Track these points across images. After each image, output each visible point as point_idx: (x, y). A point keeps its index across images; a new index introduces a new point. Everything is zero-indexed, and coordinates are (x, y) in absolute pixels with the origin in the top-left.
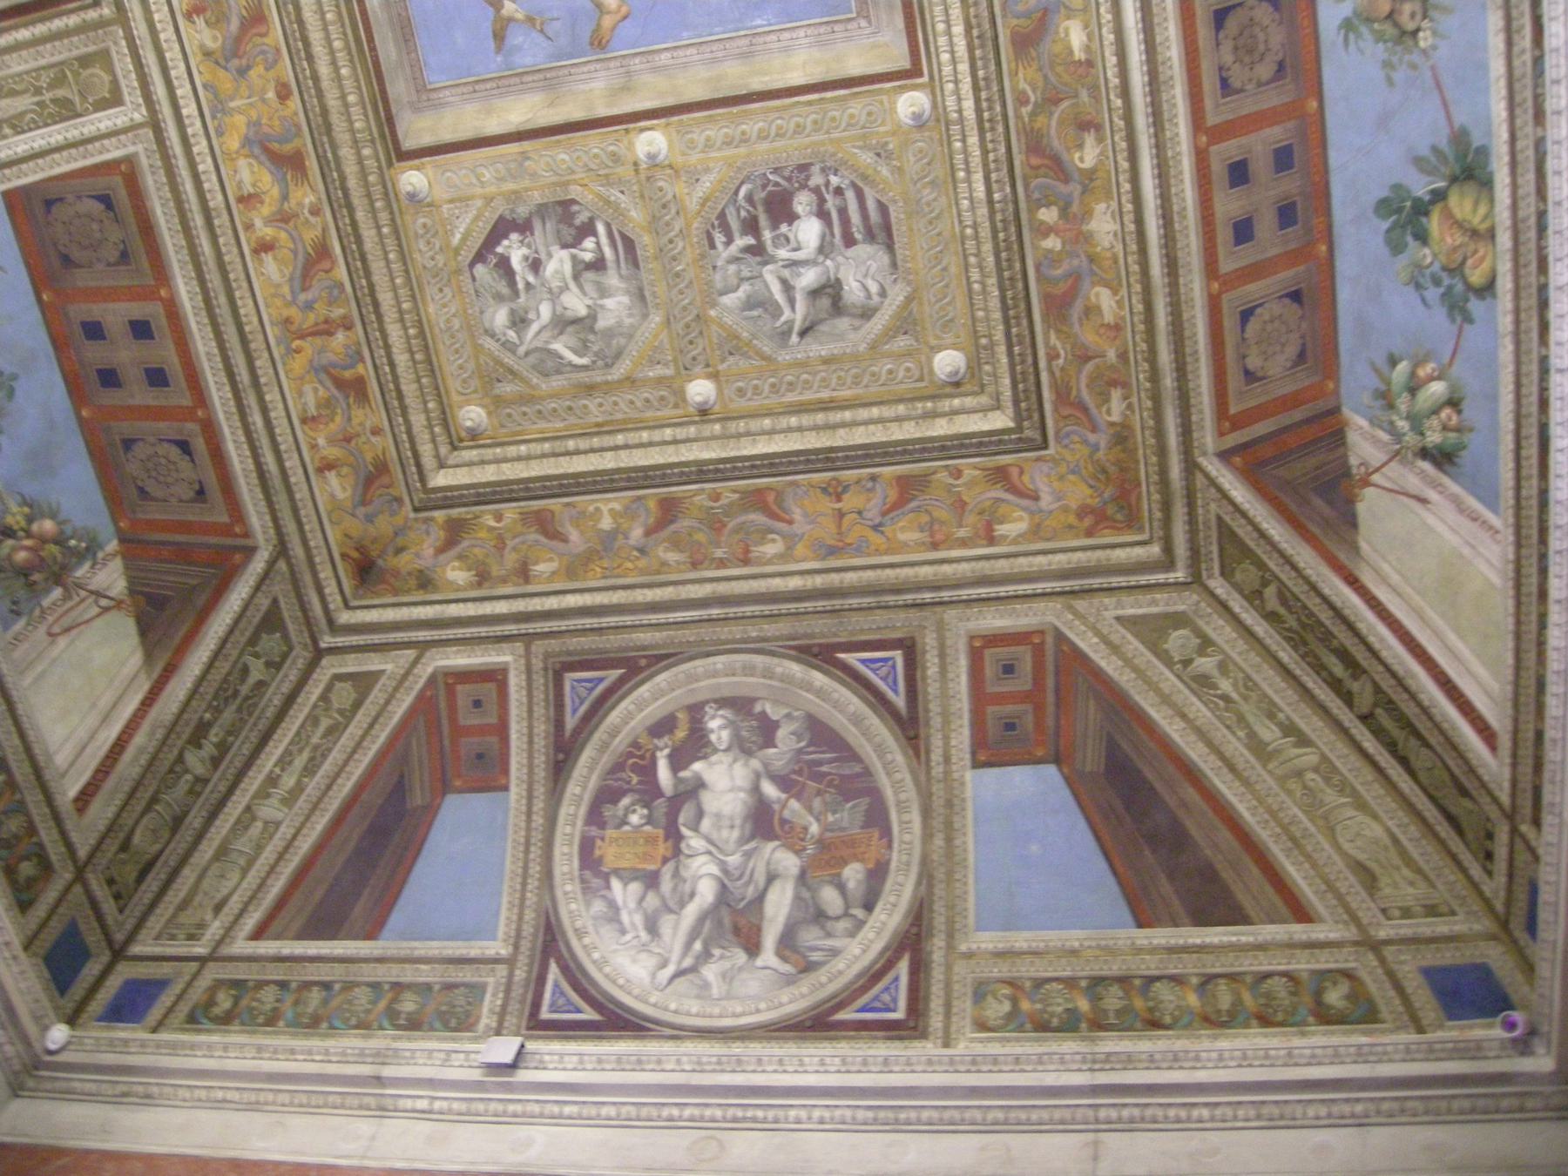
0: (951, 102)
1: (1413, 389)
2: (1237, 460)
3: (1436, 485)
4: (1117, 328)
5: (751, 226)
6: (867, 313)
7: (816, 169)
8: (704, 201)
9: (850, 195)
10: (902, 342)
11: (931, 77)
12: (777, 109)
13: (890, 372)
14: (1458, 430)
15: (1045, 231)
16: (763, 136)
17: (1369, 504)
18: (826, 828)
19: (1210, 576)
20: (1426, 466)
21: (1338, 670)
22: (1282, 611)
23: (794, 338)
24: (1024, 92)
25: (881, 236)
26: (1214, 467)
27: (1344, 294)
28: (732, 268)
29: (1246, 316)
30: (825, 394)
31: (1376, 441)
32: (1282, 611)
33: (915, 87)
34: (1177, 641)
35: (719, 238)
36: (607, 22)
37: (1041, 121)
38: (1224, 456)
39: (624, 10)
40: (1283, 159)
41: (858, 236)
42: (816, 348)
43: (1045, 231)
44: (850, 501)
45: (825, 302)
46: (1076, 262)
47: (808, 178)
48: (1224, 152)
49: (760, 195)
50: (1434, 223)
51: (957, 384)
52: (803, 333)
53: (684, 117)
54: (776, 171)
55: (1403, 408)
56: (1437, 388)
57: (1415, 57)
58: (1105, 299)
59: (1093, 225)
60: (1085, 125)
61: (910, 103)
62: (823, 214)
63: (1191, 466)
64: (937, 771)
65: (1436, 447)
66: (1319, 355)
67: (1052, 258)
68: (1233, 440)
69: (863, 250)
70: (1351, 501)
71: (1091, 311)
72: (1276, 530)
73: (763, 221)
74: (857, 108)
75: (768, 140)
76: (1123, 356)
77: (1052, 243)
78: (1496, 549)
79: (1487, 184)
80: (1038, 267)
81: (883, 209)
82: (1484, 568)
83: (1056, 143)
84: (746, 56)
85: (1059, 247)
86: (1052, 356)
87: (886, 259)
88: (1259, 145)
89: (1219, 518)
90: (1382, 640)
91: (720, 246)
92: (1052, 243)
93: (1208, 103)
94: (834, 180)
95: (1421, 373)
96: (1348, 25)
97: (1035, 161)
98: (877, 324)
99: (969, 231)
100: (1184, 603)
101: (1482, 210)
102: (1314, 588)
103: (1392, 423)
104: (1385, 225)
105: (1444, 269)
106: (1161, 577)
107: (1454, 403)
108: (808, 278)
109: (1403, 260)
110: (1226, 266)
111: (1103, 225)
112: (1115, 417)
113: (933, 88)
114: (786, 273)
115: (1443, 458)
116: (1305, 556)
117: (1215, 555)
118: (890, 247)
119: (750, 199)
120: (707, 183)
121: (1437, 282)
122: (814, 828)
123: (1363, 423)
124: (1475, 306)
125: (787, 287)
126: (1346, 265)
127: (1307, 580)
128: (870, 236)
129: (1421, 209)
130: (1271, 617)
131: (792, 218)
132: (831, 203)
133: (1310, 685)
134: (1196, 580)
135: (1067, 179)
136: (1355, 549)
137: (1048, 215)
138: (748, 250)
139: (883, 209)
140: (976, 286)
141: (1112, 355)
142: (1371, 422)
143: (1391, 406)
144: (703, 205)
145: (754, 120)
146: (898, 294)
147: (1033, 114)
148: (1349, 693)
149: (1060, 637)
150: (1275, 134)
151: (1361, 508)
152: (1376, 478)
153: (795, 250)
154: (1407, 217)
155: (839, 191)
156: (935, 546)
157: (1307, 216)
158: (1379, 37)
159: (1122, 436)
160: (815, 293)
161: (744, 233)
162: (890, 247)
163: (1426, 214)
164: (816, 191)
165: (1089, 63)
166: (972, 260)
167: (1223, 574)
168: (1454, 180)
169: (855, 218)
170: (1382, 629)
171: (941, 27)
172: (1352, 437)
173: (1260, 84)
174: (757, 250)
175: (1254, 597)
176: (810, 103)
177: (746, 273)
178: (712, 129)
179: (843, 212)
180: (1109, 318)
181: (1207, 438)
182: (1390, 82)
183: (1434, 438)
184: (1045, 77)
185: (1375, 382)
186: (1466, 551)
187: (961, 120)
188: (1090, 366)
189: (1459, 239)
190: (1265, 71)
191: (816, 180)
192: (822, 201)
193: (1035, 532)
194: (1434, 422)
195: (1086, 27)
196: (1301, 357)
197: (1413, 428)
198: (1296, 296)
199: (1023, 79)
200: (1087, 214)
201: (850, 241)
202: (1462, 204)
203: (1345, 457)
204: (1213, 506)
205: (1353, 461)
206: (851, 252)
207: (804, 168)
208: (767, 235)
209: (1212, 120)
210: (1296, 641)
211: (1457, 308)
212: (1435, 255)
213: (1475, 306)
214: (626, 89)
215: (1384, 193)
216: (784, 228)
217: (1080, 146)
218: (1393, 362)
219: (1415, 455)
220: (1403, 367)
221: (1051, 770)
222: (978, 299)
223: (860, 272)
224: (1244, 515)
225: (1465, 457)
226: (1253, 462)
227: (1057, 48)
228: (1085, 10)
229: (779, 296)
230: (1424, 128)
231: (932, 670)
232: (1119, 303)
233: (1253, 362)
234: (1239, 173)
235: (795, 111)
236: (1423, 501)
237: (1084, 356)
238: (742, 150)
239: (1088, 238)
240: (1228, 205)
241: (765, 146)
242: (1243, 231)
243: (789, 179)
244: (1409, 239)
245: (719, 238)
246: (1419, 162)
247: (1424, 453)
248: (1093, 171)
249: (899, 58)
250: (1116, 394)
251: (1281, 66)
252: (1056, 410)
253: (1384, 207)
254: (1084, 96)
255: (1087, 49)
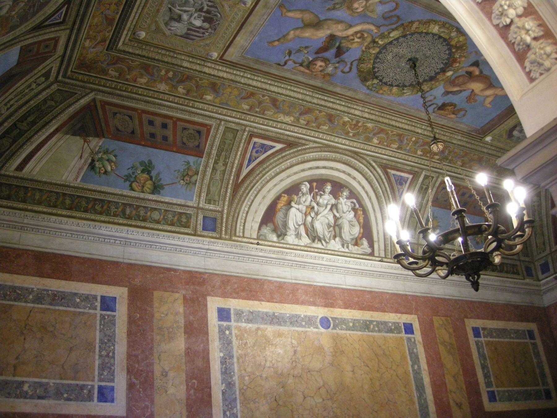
0: (209, 65)
1: (109, 160)
2: (93, 104)
3: (85, 162)
4: (135, 81)
5: (208, 12)
6: (166, 24)
7: (213, 31)
8: (223, 6)
9: (201, 35)
10: (153, 27)
11: (217, 61)
12: (233, 32)
13: (146, 22)
14: (100, 172)
15: (167, 72)
16: (229, 25)
17: (78, 141)
18: (13, 17)
19: (58, 86)
20: (90, 161)
21: (30, 119)
22: (47, 106)
23: (170, 6)
24: (202, 80)
25: (185, 36)
26: (91, 96)
27: (132, 146)
28: (200, 2)
29: (130, 117)
30: (148, 5)
31: (95, 146)
32: (47, 106)
33: (217, 57)
34: (43, 79)
35: (210, 4)
36: (284, 11)
37: (194, 82)
38: (94, 100)
39: (284, 15)
40: (165, 138)
41: (189, 32)
42: (163, 10)
43: (167, 72)
44: (113, 7)
45: (176, 17)
46: (156, 76)
47: (212, 29)
48: (170, 123)
49: (215, 18)
50: (145, 176)
51: (134, 34)
52: (170, 9)
53: (248, 13)
54: (219, 24)
55: (104, 157)
56: (109, 168)
57: (179, 179)
58: (143, 80)
59: (164, 84)
60: (188, 92)
61: (215, 55)
62: (200, 28)
63: (92, 90)
64: (23, 38)
65: (95, 165)
66: (118, 135)
67: (159, 70)
68: (98, 104)
69: (185, 31)
70: (79, 135)
71: (142, 76)
72: (71, 110)
73: (208, 15)
74: (222, 45)
75: (226, 28)
76: (127, 80)
77: (163, 73)
78: (72, 179)
79: (153, 193)
80: (158, 67)
81: (193, 39)
82: (66, 174)
83: (187, 83)
84: (251, 32)
85: (161, 74)
86: (133, 61)
87: (179, 34)
88: (169, 133)
89: (76, 93)
90: (41, 136)
91: (208, 3)
92: (163, 73)
93: (182, 123)
94: (207, 34)
95: (113, 164)
96: (188, 163)
97: (185, 76)
98: (162, 26)
99: (176, 56)
100: (52, 79)
101: (148, 190)
102: (54, 118)
103: (100, 152)
104: (146, 162)
105: (136, 176)
106: (61, 74)
107: (106, 172)
108: (185, 17)
109: (138, 165)
110: (144, 116)
111: (163, 87)
112: (110, 72)
113: (215, 62)
114: (190, 13)
115: (92, 166)
116: (63, 117)
117: (64, 89)
118: (181, 36)
119: (216, 15)
120: (227, 8)
121: (133, 173)
122: (14, 13)
123: (100, 144)
124: (128, 183)
125: (185, 11)
126: (139, 148)
127: (57, 116)
128: (187, 34)
129: (149, 173)
130: (45, 101)
131: (204, 21)
132: (202, 31)
133: (24, 109)
134: (56, 80)
135: (177, 82)
136: (67, 133)
137: (170, 74)
138: (203, 8)
139: (193, 39)
140: (160, 51)
141: (128, 77)
142: (100, 146)
143: (104, 153)
144: (222, 5)
145: (234, 26)
146: (168, 32)
147: (196, 81)
148: (22, 122)
149: (51, 56)
150: (171, 138)
151: (78, 138)
152: (86, 144)
153: (195, 18)
154: (147, 168)
155: (203, 33)
156: (90, 26)
157: (151, 141)
158: (185, 170)
159: (104, 72)
160: (180, 16)
161: (208, 10)
162: (181, 36)
163: (148, 174)
164: (207, 29)
165: (201, 98)
166: (168, 53)
167: (58, 89)
168: (154, 183)
169: (194, 33)
170: (44, 137)
171: (228, 70)
172: (97, 139)
173: (182, 137)
174: (201, 10)
175: (51, 97)
176: (230, 38)
177: (196, 4)
178: (239, 17)
179: (198, 32)
180: (139, 79)
181: (100, 97)
182: (175, 171)
183: (97, 164)
184: (203, 87)
185: (111, 150)
186: (69, 169)
187: (204, 65)
188: (126, 69)
189: (142, 182)
190: (185, 140)
191: (210, 30)
192: (203, 29)
193: (84, 48)
194: (101, 166)
195: (210, 100)
196: (118, 130)
197: (99, 158)
198: (133, 132)
199: (205, 82)
200: (167, 84)
201: (188, 29)
202: (149, 184)
203: (92, 137)
204: (79, 93)
205: (91, 138)
206: (186, 28)
207: (215, 29)
208: (203, 14)
209: (178, 123)
210: (37, 108)
211: (127, 178)
212: (139, 174)
213: (128, 183)
214: (265, 6)
215: (153, 164)
216: (202, 18)
217: (184, 89)
218: (115, 156)
219: (93, 157)
220: (114, 159)
221: (15, 64)
222: (156, 50)
223: (179, 28)
224: (76, 101)
225: (92, 173)
226: (91, 108)
227: (208, 92)
228: (214, 102)
229: (184, 8)
230: (166, 179)
231: (53, 29)
232: (141, 84)
233: (118, 116)
234: (164, 126)
235: (230, 35)
236: (81, 157)
237: (130, 69)
238: (229, 20)
239: (161, 82)
240: (158, 121)
241: (227, 24)
242: (151, 123)
243: (214, 25)
244: (143, 168)
245: (210, 4)
246: (158, 174)
247: (93, 160)
248: (177, 90)
249: (226, 57)
250: (117, 74)
251: (184, 144)
252: (117, 56)
253: (150, 162)
254: (195, 94)
255: (205, 99)
